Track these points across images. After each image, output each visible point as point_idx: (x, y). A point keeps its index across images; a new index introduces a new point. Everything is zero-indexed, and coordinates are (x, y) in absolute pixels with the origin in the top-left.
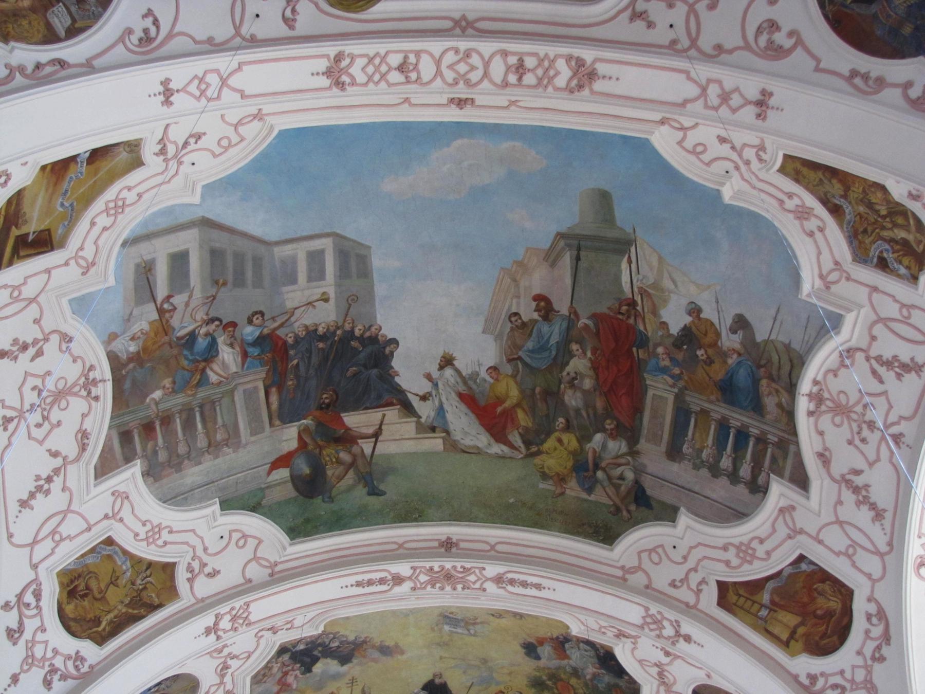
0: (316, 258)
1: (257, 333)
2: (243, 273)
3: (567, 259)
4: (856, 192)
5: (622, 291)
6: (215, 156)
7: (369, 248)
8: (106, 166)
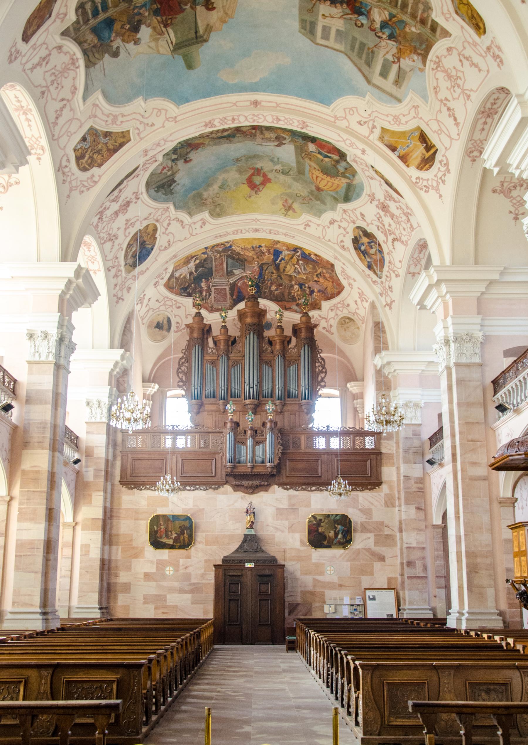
0: (326, 36)
1: (360, 18)
2: (360, 47)
3: (201, 31)
4: (105, 154)
5: (173, 29)
6: (357, 108)
7: (300, 31)
8: (393, 141)
